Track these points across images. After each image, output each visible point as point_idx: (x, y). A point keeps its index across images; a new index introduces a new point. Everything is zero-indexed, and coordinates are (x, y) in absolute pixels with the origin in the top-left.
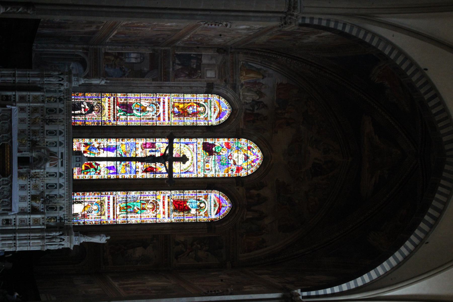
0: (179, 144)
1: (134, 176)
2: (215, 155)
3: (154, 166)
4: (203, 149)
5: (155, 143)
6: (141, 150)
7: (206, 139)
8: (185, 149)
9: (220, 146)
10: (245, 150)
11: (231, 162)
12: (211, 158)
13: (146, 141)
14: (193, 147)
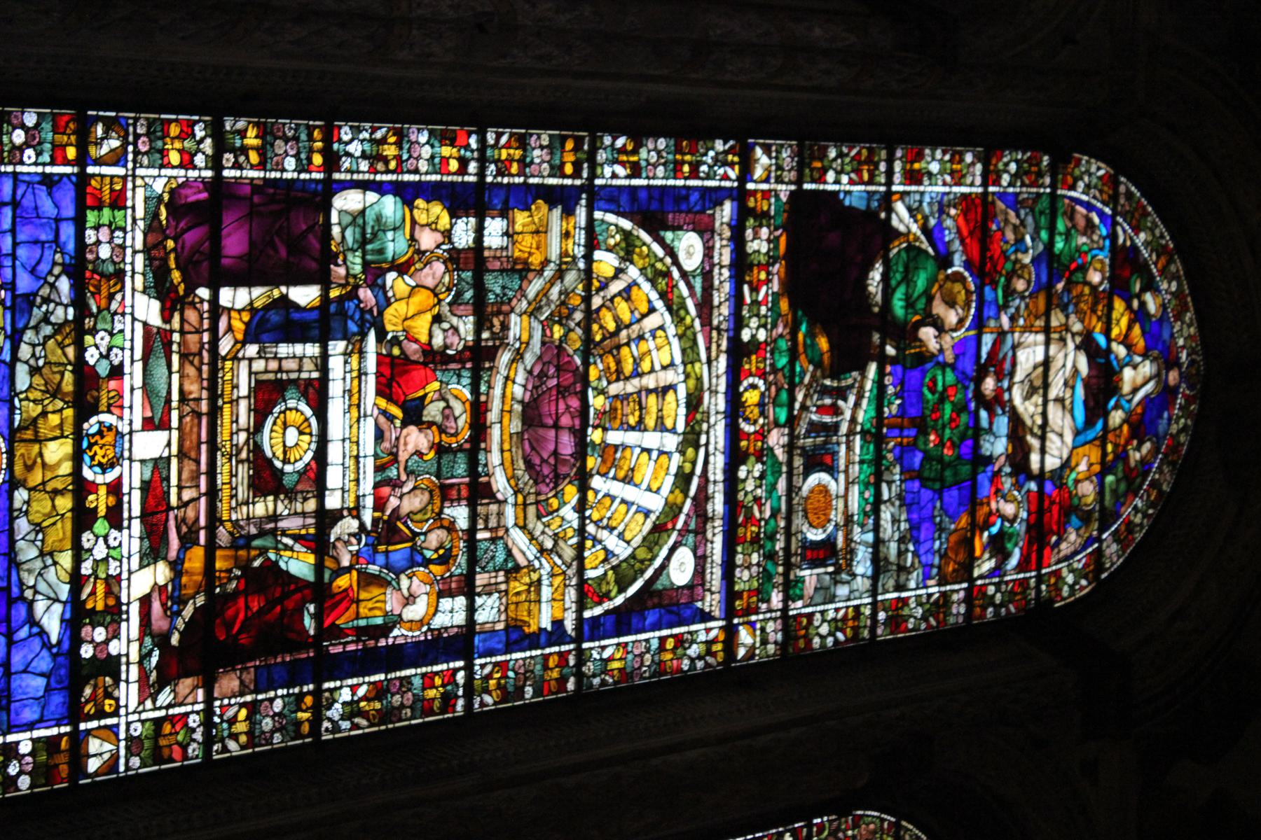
0: (581, 214)
1: (52, 743)
2: (883, 360)
3: (300, 565)
4: (791, 288)
5: (331, 188)
6: (149, 310)
7: (823, 155)
8: (626, 294)
9: (925, 245)
10: (1094, 288)
11: (997, 446)
12: (852, 399)
13: (215, 163)
14: (708, 252)
